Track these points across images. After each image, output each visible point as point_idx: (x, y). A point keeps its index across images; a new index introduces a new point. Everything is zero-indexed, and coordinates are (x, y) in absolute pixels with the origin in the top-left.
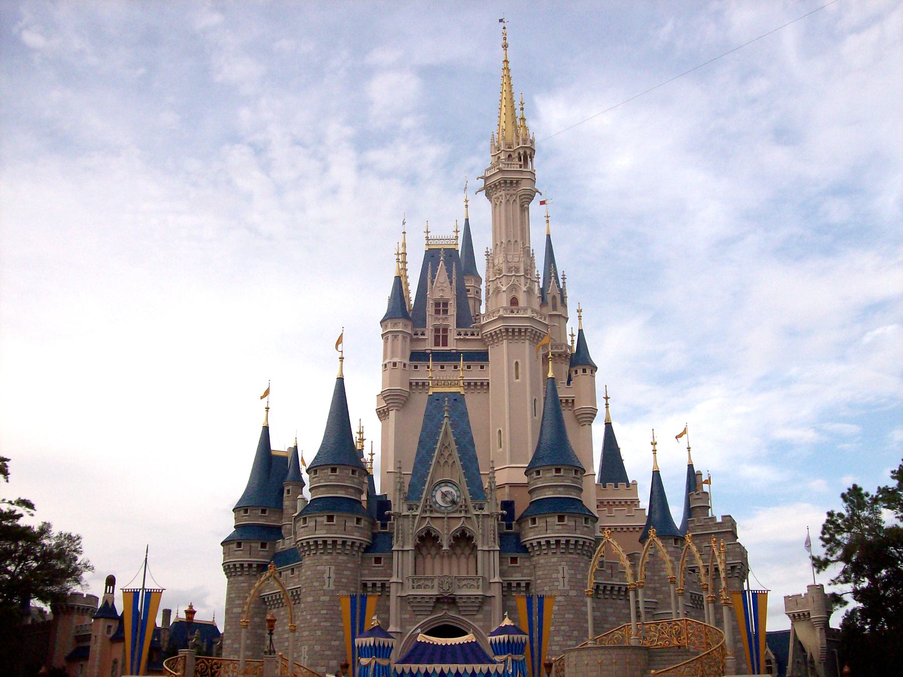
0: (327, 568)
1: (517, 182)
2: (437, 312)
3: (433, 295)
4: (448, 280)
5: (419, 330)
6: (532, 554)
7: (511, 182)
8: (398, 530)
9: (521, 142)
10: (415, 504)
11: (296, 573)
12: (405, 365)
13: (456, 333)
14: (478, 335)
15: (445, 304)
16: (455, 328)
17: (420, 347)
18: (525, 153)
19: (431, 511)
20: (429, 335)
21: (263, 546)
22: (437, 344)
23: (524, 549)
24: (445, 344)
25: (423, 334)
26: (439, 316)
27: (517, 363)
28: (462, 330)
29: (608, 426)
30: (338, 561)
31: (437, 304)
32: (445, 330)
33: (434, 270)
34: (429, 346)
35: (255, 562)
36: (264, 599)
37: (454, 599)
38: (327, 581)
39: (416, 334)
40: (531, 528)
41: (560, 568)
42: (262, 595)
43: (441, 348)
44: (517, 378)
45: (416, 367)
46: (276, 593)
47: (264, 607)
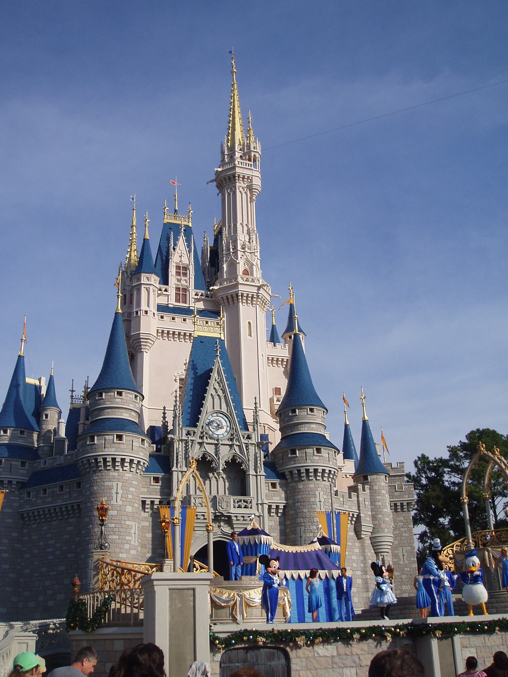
0: (115, 484)
1: (248, 177)
2: (178, 274)
3: (175, 260)
5: (164, 287)
6: (289, 480)
8: (177, 454)
10: (192, 431)
11: (66, 490)
12: (154, 314)
13: (194, 293)
14: (212, 297)
15: (186, 268)
16: (193, 289)
17: (163, 301)
18: (255, 155)
19: (207, 438)
20: (172, 292)
21: (23, 464)
22: (177, 300)
25: (166, 290)
26: (179, 278)
27: (249, 323)
30: (124, 478)
31: (178, 267)
32: (185, 290)
33: (176, 239)
34: (173, 302)
35: (15, 480)
36: (23, 515)
37: (229, 517)
38: (114, 495)
40: (291, 458)
41: (317, 493)
42: (20, 510)
44: (250, 335)
45: (162, 317)
46: (34, 510)
47: (21, 522)
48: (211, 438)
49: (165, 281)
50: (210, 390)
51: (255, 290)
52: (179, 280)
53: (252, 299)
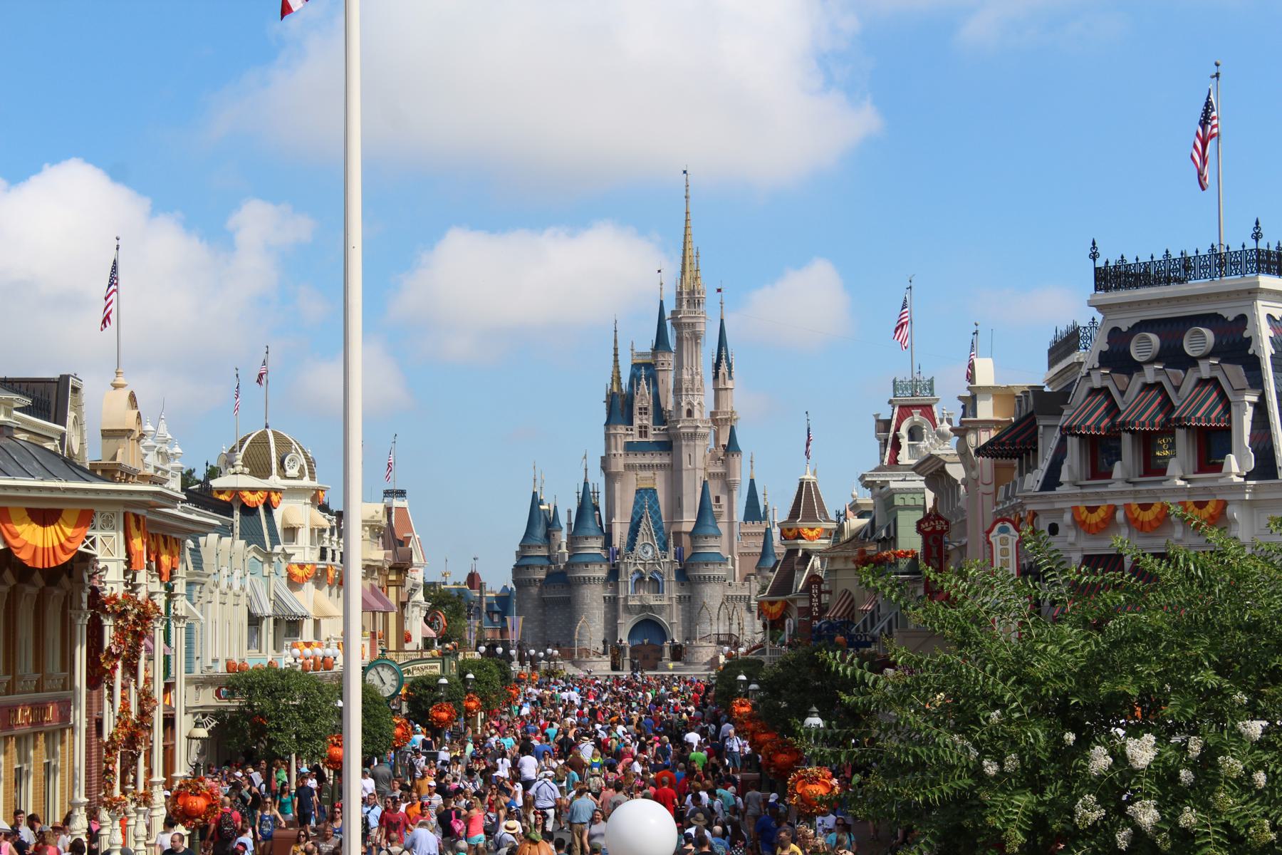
2: (641, 414)
3: (637, 405)
4: (647, 392)
7: (689, 324)
9: (696, 293)
17: (629, 439)
20: (636, 431)
22: (641, 436)
23: (688, 579)
24: (646, 436)
25: (632, 430)
28: (657, 427)
29: (752, 481)
31: (640, 409)
33: (638, 384)
34: (637, 439)
39: (627, 430)
43: (644, 440)
48: (642, 560)
49: (630, 422)
50: (641, 530)
51: (692, 430)
52: (641, 420)
53: (693, 436)
